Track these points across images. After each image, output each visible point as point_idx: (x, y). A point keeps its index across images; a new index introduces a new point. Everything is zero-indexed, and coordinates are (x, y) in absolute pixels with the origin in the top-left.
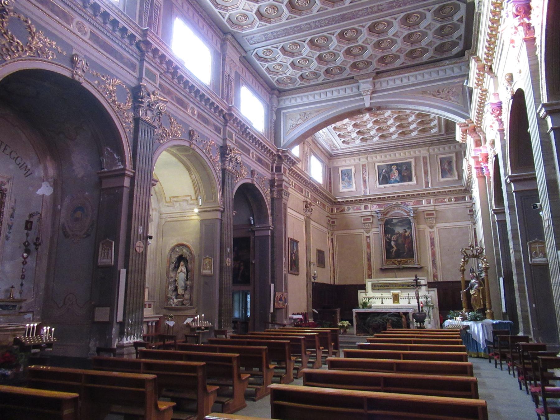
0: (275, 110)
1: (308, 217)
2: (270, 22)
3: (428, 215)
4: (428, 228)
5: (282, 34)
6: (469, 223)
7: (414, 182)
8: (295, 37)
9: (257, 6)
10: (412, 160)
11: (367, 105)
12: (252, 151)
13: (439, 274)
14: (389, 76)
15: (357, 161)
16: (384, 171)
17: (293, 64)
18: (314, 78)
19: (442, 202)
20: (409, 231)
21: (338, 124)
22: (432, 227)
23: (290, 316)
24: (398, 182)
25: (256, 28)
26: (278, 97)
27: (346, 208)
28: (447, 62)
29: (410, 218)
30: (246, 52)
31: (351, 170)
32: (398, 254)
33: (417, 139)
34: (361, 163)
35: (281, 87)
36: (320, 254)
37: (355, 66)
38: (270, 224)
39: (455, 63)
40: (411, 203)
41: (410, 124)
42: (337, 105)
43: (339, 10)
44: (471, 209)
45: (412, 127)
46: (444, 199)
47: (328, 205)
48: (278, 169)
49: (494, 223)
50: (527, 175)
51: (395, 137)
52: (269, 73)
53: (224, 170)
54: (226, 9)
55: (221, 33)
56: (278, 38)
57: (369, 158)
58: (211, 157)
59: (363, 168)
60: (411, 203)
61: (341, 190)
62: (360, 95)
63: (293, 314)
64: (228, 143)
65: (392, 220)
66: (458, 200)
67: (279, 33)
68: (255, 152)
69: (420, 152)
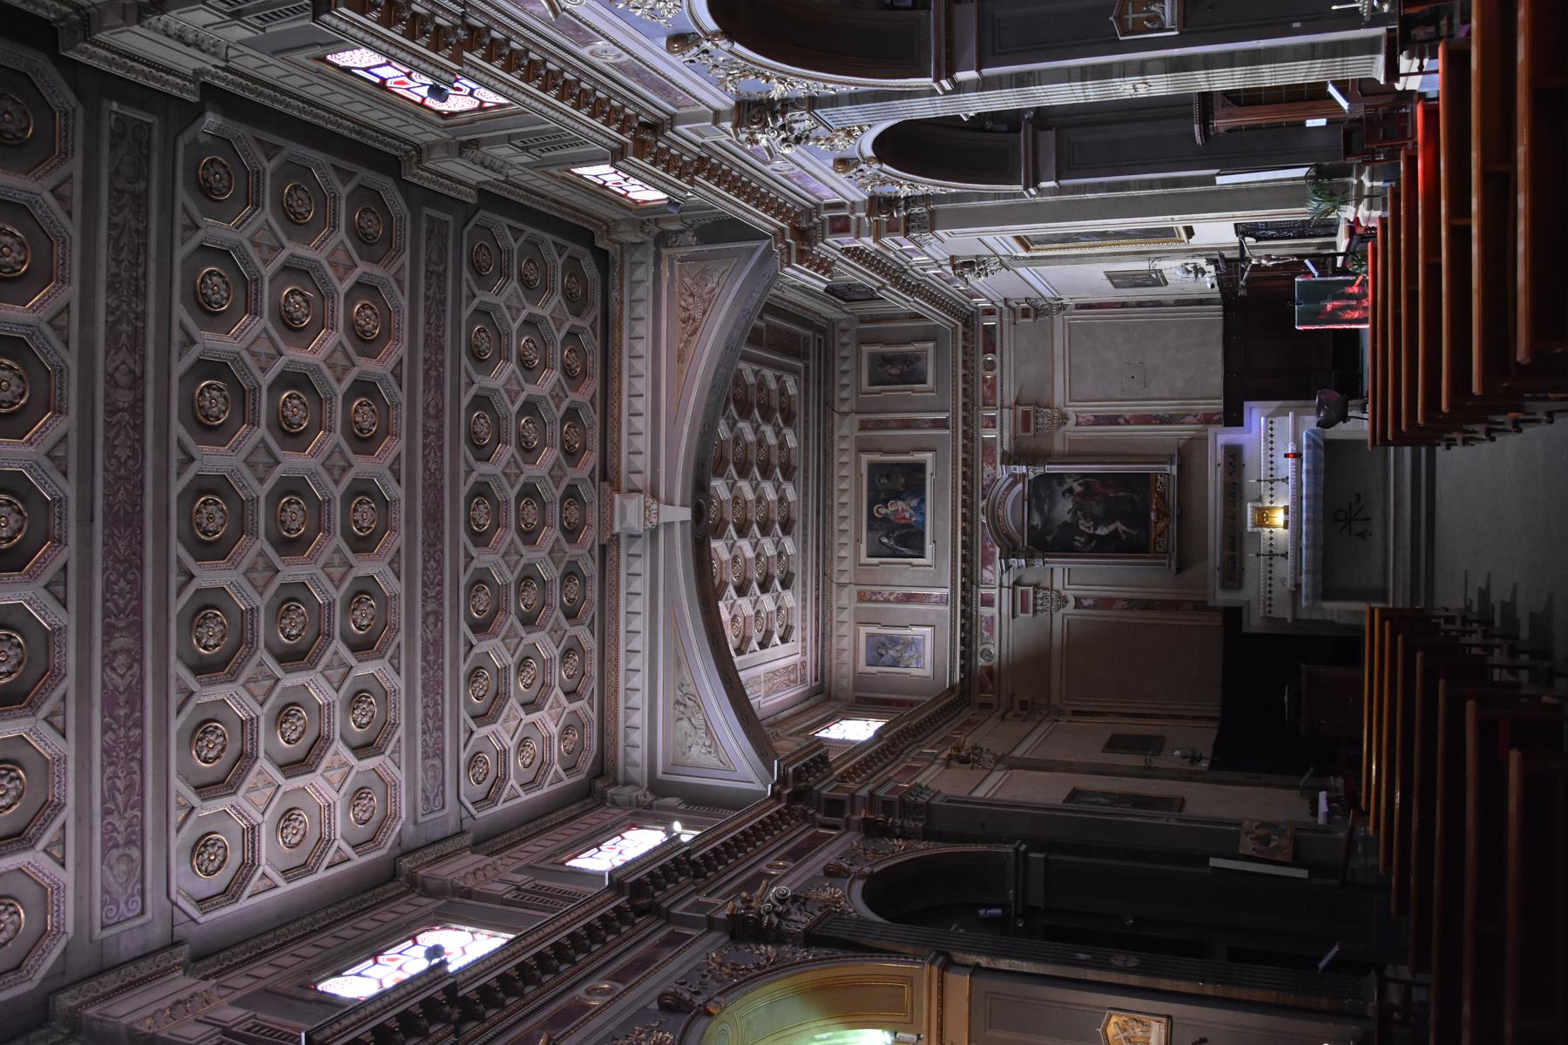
0: (650, 798)
1: (999, 760)
2: (395, 725)
3: (1026, 428)
4: (1064, 428)
5: (436, 704)
6: (1058, 319)
7: (928, 457)
8: (455, 668)
9: (338, 745)
10: (866, 458)
11: (686, 514)
12: (763, 867)
13: (1202, 407)
14: (619, 448)
15: (845, 616)
16: (885, 540)
17: (530, 706)
18: (583, 660)
19: (992, 387)
21: (732, 641)
22: (1064, 418)
23: (1321, 820)
24: (923, 501)
25: (401, 776)
26: (615, 783)
27: (981, 662)
28: (614, 294)
29: (1032, 476)
30: (462, 832)
31: (869, 636)
32: (1138, 518)
33: (806, 437)
34: (854, 604)
35: (586, 764)
36: (1115, 744)
37: (571, 533)
38: (1008, 849)
39: (621, 279)
40: (989, 469)
41: (761, 442)
42: (672, 603)
43: (410, 521)
44: (1020, 314)
45: (771, 439)
46: (985, 380)
47: (966, 714)
48: (835, 807)
49: (1061, 190)
50: (938, 41)
51: (791, 494)
52: (540, 786)
53: (810, 939)
54: (324, 842)
55: (391, 885)
56: (442, 720)
57: (843, 580)
58: (758, 967)
59: (870, 601)
60: (989, 469)
61: (927, 671)
62: (654, 533)
63: (1315, 812)
64: (722, 915)
65: (1031, 528)
66: (993, 345)
67: (431, 712)
68: (770, 861)
69: (844, 438)
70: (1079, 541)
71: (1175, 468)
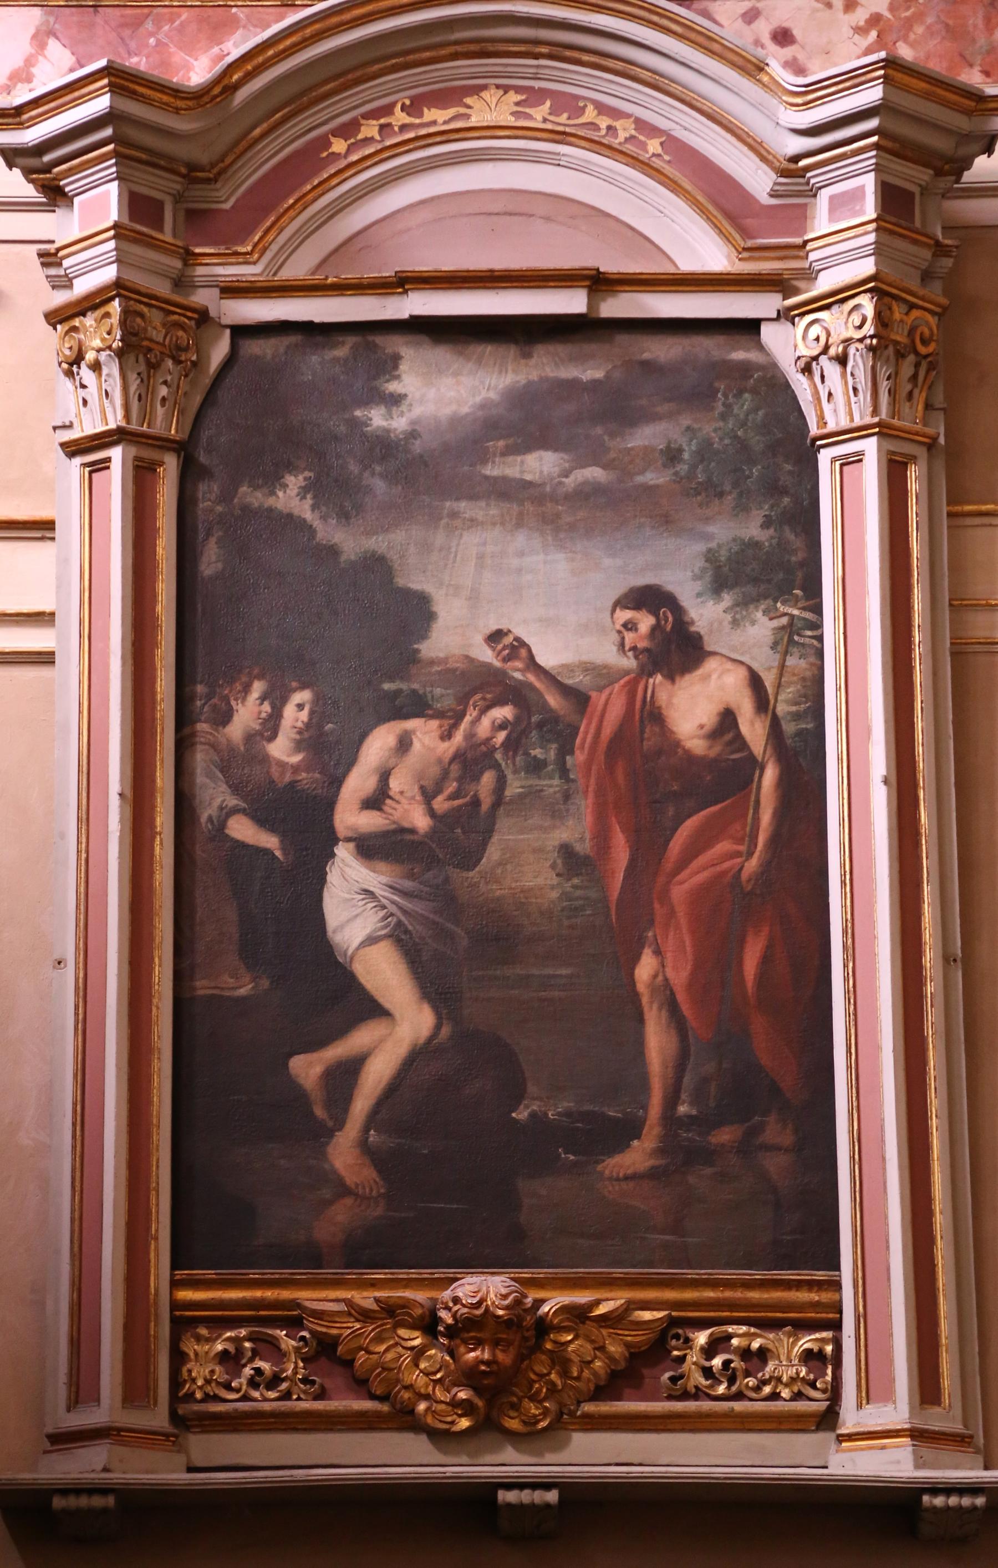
20: (740, 639)
29: (785, 344)
70: (272, 723)
71: (894, 1464)
